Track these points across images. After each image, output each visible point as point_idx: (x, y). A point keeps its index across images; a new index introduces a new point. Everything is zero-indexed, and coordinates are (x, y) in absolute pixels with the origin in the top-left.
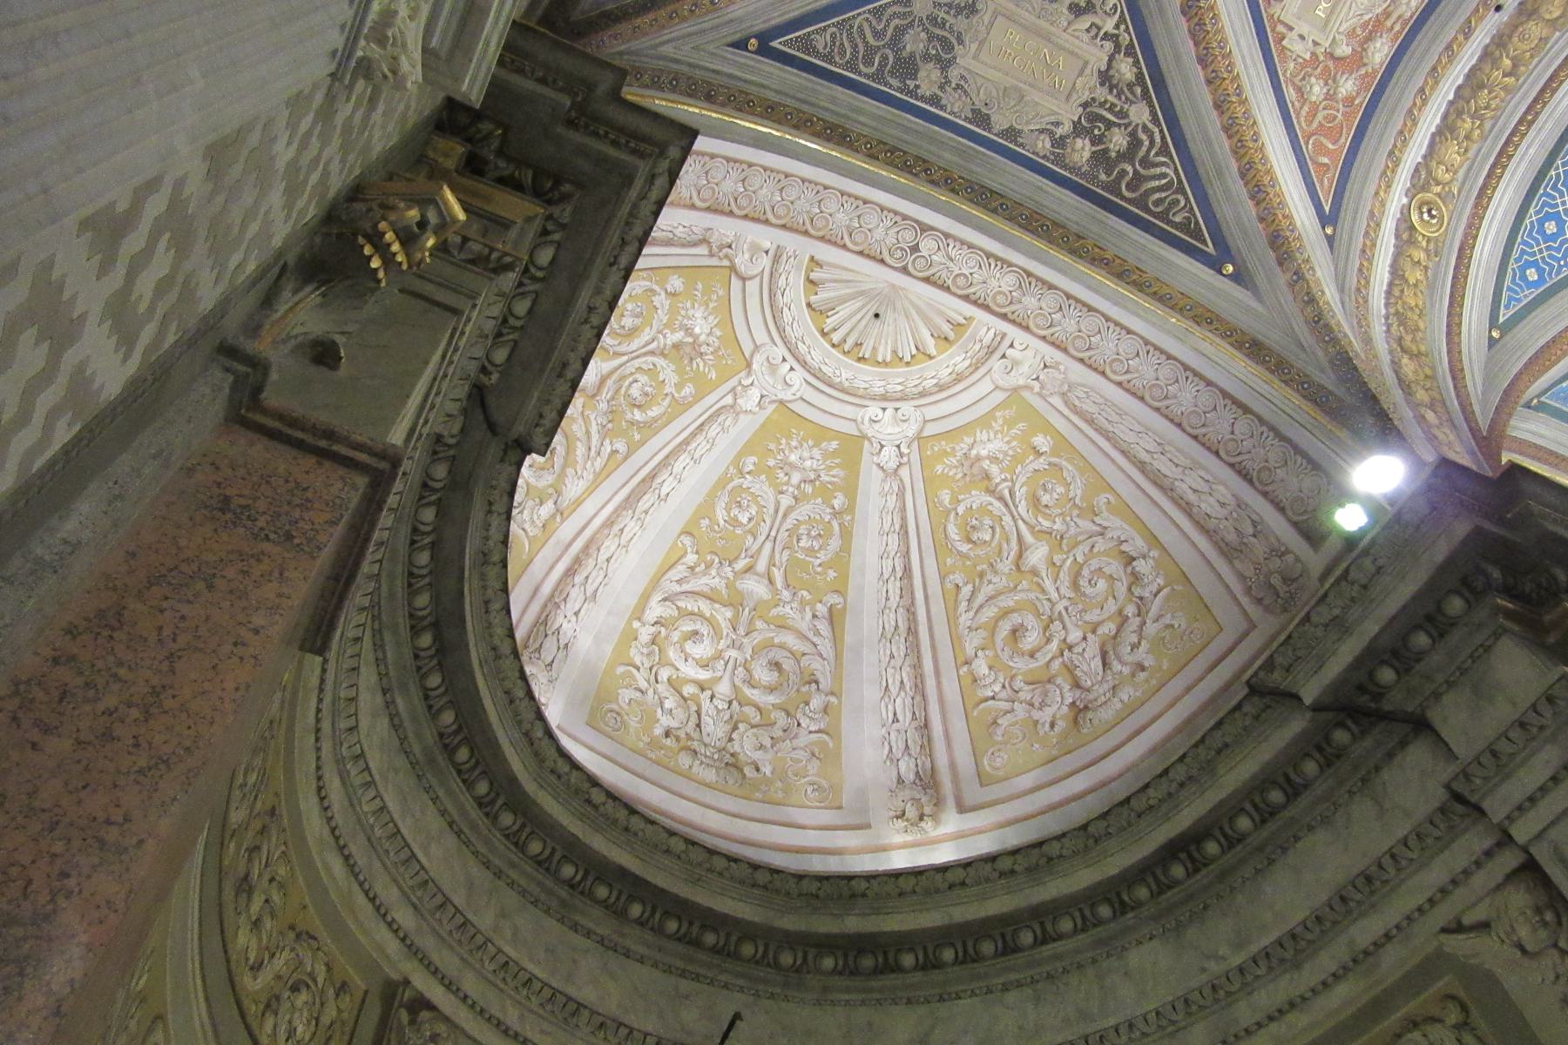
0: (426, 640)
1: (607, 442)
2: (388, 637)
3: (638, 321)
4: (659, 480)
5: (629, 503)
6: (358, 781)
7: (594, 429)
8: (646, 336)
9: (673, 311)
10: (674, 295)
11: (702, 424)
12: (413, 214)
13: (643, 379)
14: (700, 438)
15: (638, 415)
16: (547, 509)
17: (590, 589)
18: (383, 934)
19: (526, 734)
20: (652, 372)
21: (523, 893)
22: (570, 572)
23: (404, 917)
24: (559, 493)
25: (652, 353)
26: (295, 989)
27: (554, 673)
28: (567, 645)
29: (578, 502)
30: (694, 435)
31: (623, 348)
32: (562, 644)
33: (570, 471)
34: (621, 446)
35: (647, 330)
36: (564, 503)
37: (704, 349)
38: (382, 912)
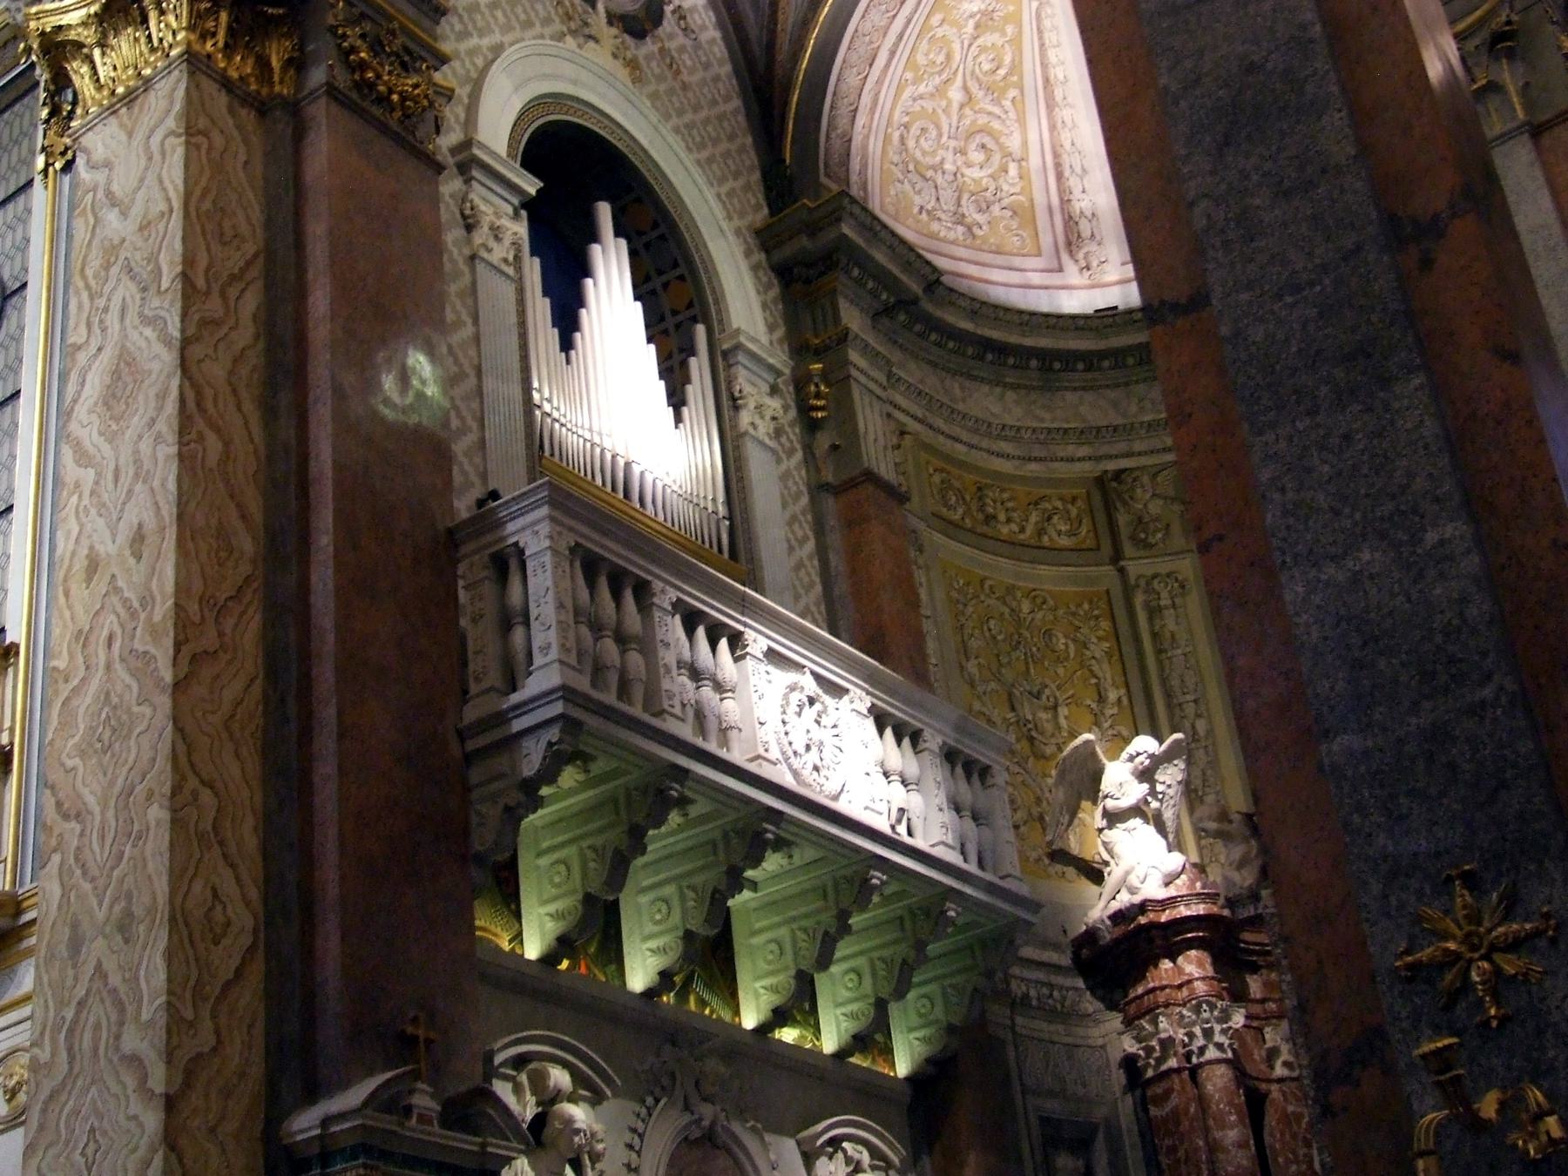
0: (989, 357)
1: (1004, 102)
2: (975, 373)
3: (944, 51)
4: (1052, 77)
5: (1051, 105)
6: (1013, 433)
7: (990, 108)
8: (956, 46)
9: (954, 24)
10: (943, 21)
11: (1038, 29)
12: (813, 388)
13: (982, 58)
14: (1046, 35)
15: (1002, 72)
16: (1013, 169)
17: (1078, 170)
18: (1078, 467)
19: (1077, 329)
20: (983, 50)
21: (1145, 380)
22: (1060, 176)
23: (1083, 451)
24: (1010, 154)
25: (970, 45)
26: (1049, 518)
27: (1098, 238)
28: (1093, 214)
29: (1025, 143)
30: (1041, 38)
31: (954, 67)
32: (1090, 217)
33: (1002, 140)
34: (1013, 93)
35: (954, 45)
36: (1018, 154)
37: (990, 8)
38: (1071, 460)
